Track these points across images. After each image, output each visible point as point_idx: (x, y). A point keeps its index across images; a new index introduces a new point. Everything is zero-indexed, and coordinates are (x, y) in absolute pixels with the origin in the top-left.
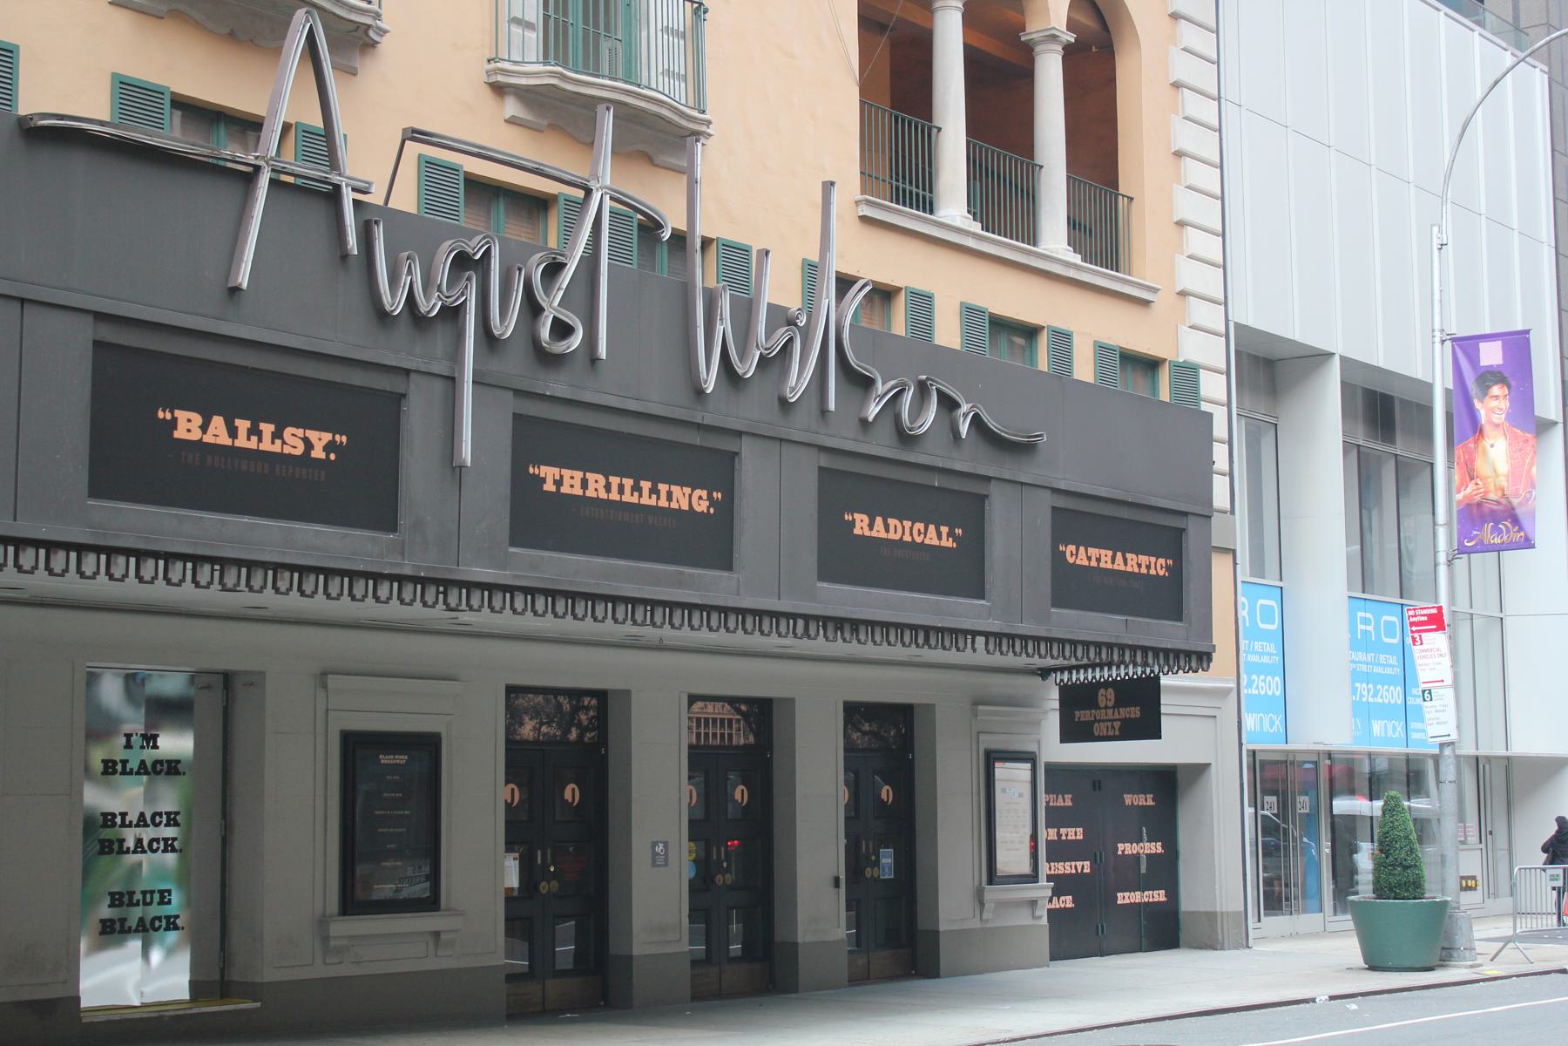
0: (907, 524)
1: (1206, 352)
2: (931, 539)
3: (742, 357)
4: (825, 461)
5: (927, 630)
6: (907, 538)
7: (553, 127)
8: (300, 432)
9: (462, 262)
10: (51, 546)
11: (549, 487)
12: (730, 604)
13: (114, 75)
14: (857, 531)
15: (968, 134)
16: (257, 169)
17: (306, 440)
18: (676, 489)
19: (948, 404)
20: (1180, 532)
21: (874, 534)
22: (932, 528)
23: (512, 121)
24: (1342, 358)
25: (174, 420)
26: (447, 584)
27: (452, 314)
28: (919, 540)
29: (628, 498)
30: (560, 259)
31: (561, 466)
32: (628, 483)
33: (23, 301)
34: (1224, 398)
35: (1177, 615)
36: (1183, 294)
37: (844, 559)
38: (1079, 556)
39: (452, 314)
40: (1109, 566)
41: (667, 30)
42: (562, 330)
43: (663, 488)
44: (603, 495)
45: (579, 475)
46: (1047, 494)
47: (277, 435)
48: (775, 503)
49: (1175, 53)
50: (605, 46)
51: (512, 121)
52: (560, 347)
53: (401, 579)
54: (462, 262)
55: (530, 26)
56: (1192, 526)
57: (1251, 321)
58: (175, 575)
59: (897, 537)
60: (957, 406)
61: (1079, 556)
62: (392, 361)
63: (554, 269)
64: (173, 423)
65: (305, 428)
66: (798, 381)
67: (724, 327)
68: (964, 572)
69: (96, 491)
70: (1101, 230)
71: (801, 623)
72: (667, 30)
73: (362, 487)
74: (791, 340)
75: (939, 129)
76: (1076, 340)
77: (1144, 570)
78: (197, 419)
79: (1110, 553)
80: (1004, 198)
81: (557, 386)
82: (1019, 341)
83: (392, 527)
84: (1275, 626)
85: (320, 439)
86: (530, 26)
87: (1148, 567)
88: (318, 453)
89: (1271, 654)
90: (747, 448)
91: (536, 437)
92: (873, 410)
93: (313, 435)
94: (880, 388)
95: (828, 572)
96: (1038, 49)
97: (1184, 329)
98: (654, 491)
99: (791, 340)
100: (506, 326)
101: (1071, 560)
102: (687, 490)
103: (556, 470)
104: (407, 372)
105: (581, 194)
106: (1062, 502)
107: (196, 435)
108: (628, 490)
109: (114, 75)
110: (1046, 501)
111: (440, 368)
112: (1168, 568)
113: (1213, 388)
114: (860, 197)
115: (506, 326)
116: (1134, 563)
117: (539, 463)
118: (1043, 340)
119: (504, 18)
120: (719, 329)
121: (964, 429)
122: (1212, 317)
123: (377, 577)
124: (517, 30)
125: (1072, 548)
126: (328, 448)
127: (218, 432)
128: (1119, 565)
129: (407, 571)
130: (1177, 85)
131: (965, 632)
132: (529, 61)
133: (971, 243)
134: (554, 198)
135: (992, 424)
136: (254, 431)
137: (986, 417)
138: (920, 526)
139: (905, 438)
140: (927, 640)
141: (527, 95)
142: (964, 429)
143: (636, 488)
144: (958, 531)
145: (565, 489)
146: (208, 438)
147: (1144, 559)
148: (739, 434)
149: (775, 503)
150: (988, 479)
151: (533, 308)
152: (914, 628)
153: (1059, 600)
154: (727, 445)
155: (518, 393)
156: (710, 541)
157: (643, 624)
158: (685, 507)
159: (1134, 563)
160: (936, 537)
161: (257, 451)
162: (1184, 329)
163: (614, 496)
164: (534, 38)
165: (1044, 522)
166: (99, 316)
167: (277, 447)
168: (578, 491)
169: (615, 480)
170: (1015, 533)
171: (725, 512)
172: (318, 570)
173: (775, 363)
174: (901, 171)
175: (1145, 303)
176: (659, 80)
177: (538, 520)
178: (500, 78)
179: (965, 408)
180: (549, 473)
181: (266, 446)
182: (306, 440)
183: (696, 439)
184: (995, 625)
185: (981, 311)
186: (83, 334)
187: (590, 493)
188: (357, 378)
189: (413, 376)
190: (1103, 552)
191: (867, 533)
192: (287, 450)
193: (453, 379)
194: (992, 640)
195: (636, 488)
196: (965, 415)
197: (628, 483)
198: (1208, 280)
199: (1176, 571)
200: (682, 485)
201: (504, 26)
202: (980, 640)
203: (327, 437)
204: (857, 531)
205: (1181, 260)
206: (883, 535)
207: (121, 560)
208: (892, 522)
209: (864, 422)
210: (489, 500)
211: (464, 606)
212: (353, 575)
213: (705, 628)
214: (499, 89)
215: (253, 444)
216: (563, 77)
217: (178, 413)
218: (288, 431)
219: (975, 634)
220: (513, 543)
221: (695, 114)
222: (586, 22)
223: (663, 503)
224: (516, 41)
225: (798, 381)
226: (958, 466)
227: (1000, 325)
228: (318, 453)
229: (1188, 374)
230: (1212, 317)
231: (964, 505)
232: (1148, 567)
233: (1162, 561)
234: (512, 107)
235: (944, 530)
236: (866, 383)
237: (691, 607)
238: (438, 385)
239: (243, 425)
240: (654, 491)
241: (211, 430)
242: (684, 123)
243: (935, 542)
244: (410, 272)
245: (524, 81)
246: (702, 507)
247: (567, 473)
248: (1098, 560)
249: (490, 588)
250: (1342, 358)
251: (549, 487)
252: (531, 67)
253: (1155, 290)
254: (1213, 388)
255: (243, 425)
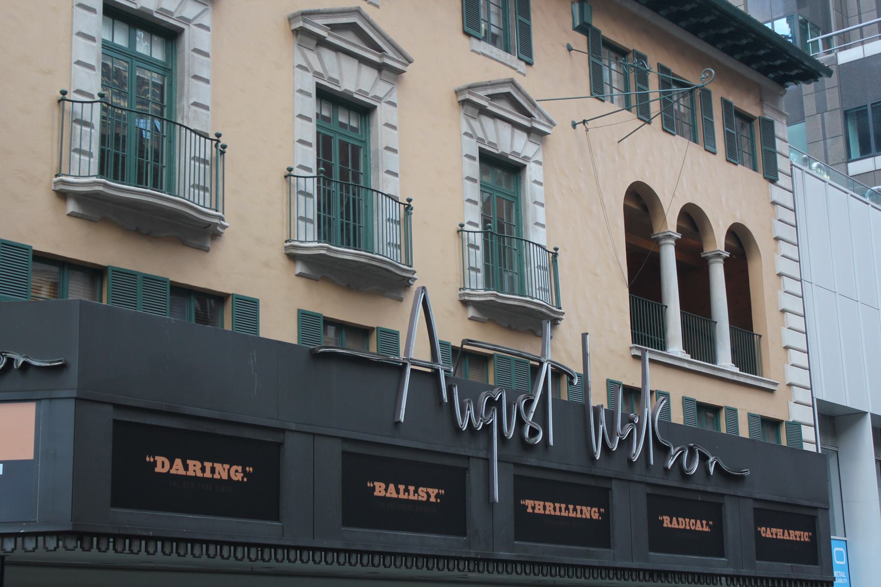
0: (687, 520)
1: (804, 415)
2: (699, 527)
3: (612, 439)
4: (649, 490)
5: (699, 575)
6: (688, 528)
7: (490, 320)
8: (425, 489)
9: (491, 402)
10: (327, 550)
11: (530, 510)
12: (611, 565)
13: (299, 310)
14: (665, 525)
15: (681, 308)
16: (405, 365)
17: (427, 493)
18: (584, 508)
19: (704, 458)
20: (814, 518)
21: (673, 526)
22: (698, 521)
23: (471, 319)
24: (872, 414)
25: (374, 487)
26: (487, 561)
27: (487, 428)
28: (693, 528)
29: (564, 514)
30: (531, 398)
31: (534, 499)
32: (563, 506)
33: (314, 434)
34: (814, 440)
35: (815, 562)
36: (790, 385)
37: (663, 540)
38: (768, 533)
39: (487, 428)
40: (782, 537)
41: (539, 267)
42: (534, 432)
43: (578, 508)
44: (553, 513)
45: (542, 503)
46: (751, 501)
47: (416, 491)
48: (628, 510)
49: (778, 257)
50: (506, 276)
51: (471, 319)
52: (532, 441)
53: (469, 559)
54: (492, 403)
55: (477, 270)
56: (820, 514)
57: (825, 398)
58: (197, 552)
59: (683, 527)
60: (708, 458)
61: (768, 533)
62: (462, 452)
63: (529, 403)
64: (374, 488)
65: (427, 487)
66: (637, 451)
67: (603, 426)
68: (713, 544)
69: (346, 522)
70: (747, 354)
71: (641, 573)
72: (539, 267)
73: (450, 516)
74: (632, 430)
75: (666, 307)
76: (739, 412)
77: (798, 539)
78: (383, 485)
79: (781, 530)
80: (699, 342)
81: (532, 460)
82: (710, 415)
83: (464, 534)
84: (844, 562)
85: (433, 492)
86: (478, 270)
87: (800, 537)
88: (433, 499)
89: (843, 578)
90: (615, 486)
91: (525, 485)
92: (671, 463)
93: (430, 490)
94: (673, 451)
95: (653, 548)
96: (711, 261)
97: (791, 404)
98: (575, 510)
99: (632, 430)
100: (510, 434)
101: (764, 535)
102: (589, 508)
103: (532, 502)
104: (468, 457)
105: (538, 364)
106: (758, 505)
107: (383, 494)
108: (563, 510)
109: (299, 310)
110: (751, 504)
111: (482, 454)
112: (810, 537)
113: (809, 434)
114: (632, 345)
115: (510, 434)
116: (794, 535)
117: (524, 499)
118: (723, 414)
119: (467, 266)
120: (601, 427)
121: (712, 470)
122: (804, 396)
123: (458, 559)
124: (473, 273)
125: (763, 529)
126: (437, 496)
127: (392, 493)
128: (786, 537)
129: (473, 556)
130: (780, 275)
131: (717, 575)
132: (479, 290)
133: (686, 365)
134: (492, 356)
135: (724, 467)
136: (406, 490)
137: (721, 464)
138: (693, 521)
139: (684, 476)
140: (693, 580)
141: (479, 306)
142: (712, 470)
143: (567, 509)
144: (711, 523)
145: (536, 511)
146: (388, 495)
147: (797, 533)
148: (610, 479)
149: (628, 510)
150: (723, 495)
151: (521, 423)
152: (693, 574)
153: (760, 556)
154: (605, 484)
155: (517, 465)
156: (598, 534)
157: (474, 571)
158: (589, 517)
159: (794, 535)
160: (700, 526)
161: (408, 500)
162: (791, 404)
163: (558, 513)
164: (481, 276)
165: (750, 515)
166: (345, 440)
167: (415, 498)
168: (542, 512)
169: (557, 505)
170: (736, 521)
171: (606, 517)
172: (434, 557)
173: (626, 444)
174: (647, 329)
175: (772, 391)
176: (536, 294)
177: (529, 527)
178: (466, 298)
179: (711, 459)
180: (529, 503)
181: (411, 497)
182: (427, 493)
183: (592, 483)
184: (730, 571)
185: (692, 400)
186: (337, 448)
187: (547, 512)
188: (448, 462)
189: (471, 460)
190: (778, 530)
191: (669, 526)
192: (420, 498)
193: (488, 460)
194: (729, 579)
195: (567, 509)
196: (712, 463)
197: (563, 506)
198: (802, 377)
199: (813, 538)
200: (587, 506)
201: (467, 271)
202: (723, 579)
203: (436, 491)
204: (665, 525)
205: (788, 367)
206: (677, 526)
207: (421, 560)
208: (680, 519)
209: (666, 469)
210: (505, 519)
211: (466, 570)
212: (448, 558)
213: (495, 572)
214: (465, 303)
215: (406, 497)
216: (497, 296)
217: (375, 483)
218: (420, 489)
219: (721, 575)
220: (516, 540)
221: (555, 309)
222: (500, 265)
223: (579, 516)
224: (473, 279)
225: (637, 451)
226: (710, 489)
227: (702, 408)
228: (433, 499)
229: (795, 427)
230: (804, 396)
231: (711, 509)
232: (800, 537)
233: (806, 533)
234: (471, 312)
235: (704, 522)
236: (667, 449)
237: (592, 568)
238: (481, 463)
239: (402, 487)
240: (575, 510)
241: (389, 491)
242: (552, 315)
243: (700, 529)
244: (469, 409)
245: (477, 299)
246: (596, 516)
247: (537, 503)
248: (776, 535)
249: (506, 562)
250: (872, 414)
251: (530, 510)
252: (479, 290)
253: (776, 384)
254: (809, 434)
255: (402, 487)
